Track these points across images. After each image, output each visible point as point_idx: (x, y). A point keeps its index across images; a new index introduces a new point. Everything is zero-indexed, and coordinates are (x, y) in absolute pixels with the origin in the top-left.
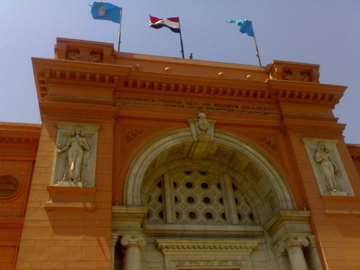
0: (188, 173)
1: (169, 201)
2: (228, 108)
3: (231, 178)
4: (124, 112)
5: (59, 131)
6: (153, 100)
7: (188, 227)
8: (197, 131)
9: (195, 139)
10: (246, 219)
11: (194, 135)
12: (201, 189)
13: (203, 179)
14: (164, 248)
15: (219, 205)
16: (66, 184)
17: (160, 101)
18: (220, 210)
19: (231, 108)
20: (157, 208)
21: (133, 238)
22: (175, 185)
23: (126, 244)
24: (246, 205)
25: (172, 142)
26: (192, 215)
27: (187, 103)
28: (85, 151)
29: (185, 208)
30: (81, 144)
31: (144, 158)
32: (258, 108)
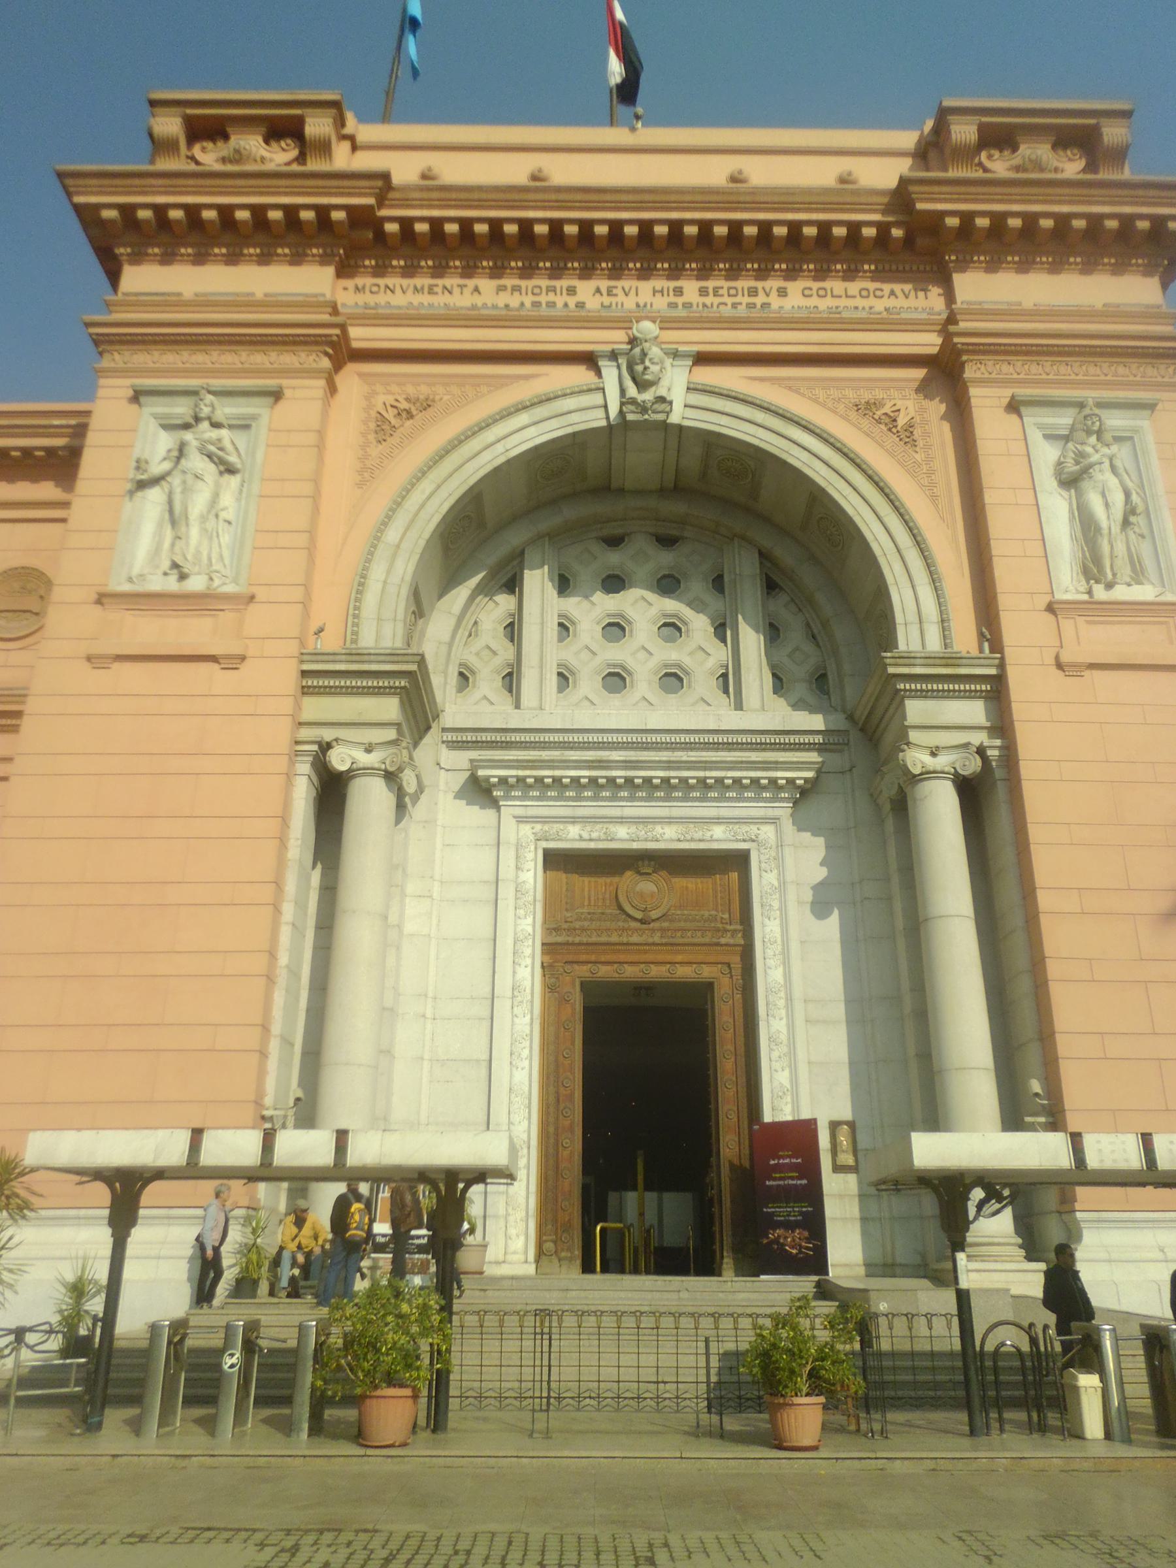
0: (614, 542)
3: (761, 554)
5: (147, 411)
7: (584, 718)
8: (623, 392)
10: (801, 690)
11: (613, 411)
14: (494, 785)
16: (158, 583)
17: (501, 289)
18: (711, 662)
19: (760, 300)
21: (369, 749)
22: (564, 585)
23: (343, 767)
24: (808, 647)
25: (532, 431)
28: (227, 476)
29: (590, 652)
30: (212, 448)
31: (427, 492)
32: (864, 294)
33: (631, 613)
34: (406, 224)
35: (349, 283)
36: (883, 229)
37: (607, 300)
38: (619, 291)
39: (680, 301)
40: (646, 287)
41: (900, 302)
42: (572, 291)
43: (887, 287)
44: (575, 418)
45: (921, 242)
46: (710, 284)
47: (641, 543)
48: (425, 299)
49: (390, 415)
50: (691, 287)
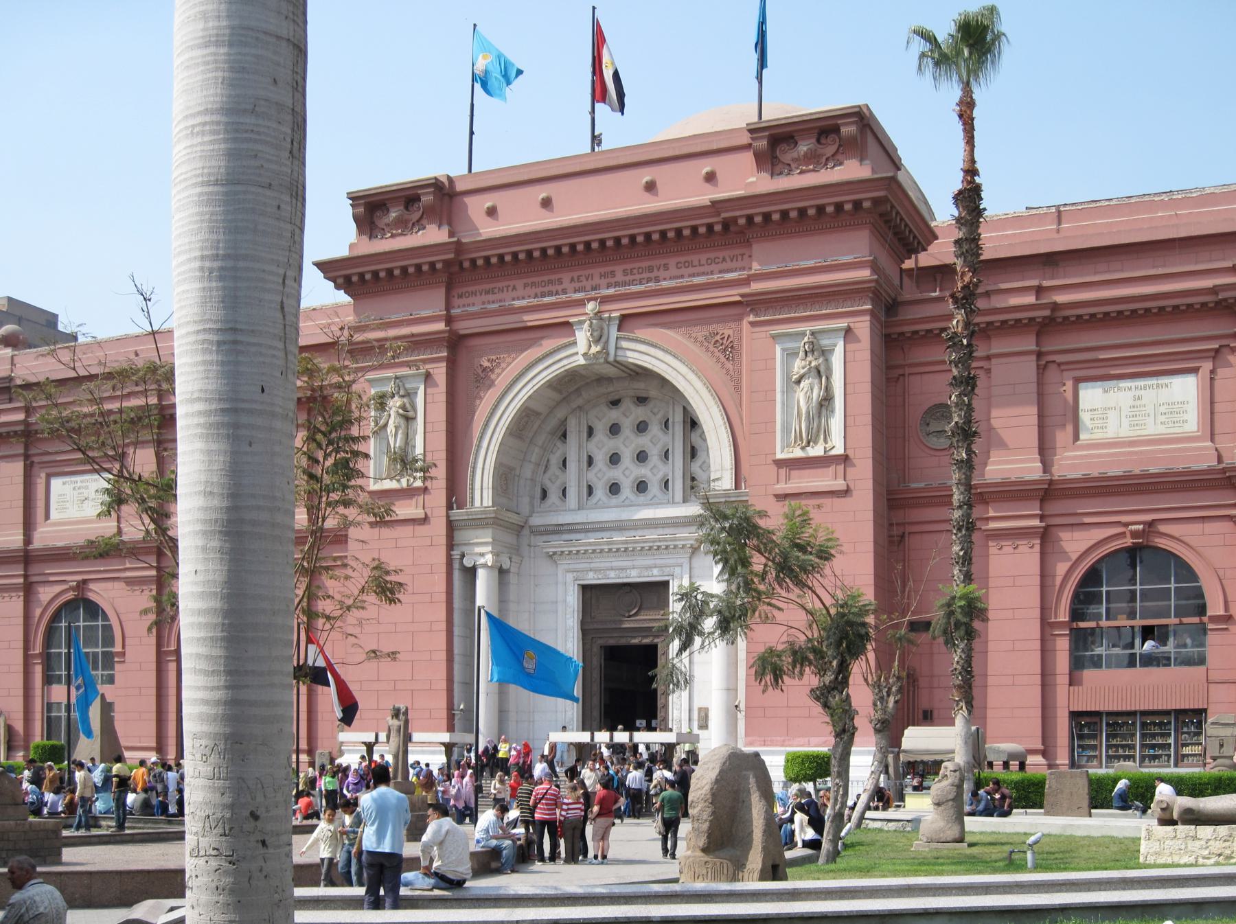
0: (615, 403)
1: (572, 465)
2: (645, 275)
4: (464, 327)
6: (514, 288)
9: (582, 361)
12: (632, 436)
13: (640, 413)
15: (660, 465)
17: (525, 285)
18: (660, 475)
19: (652, 275)
20: (558, 483)
26: (614, 489)
27: (572, 280)
32: (710, 262)
33: (622, 448)
34: (473, 261)
35: (455, 293)
36: (710, 227)
37: (577, 285)
38: (583, 278)
39: (613, 280)
40: (596, 272)
41: (729, 265)
42: (560, 281)
43: (721, 254)
44: (565, 362)
45: (732, 228)
46: (629, 266)
47: (627, 404)
48: (490, 297)
49: (480, 371)
50: (619, 270)
